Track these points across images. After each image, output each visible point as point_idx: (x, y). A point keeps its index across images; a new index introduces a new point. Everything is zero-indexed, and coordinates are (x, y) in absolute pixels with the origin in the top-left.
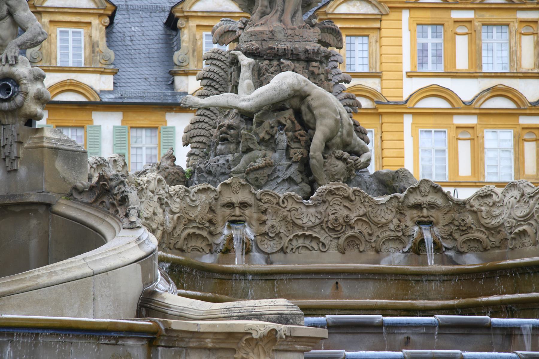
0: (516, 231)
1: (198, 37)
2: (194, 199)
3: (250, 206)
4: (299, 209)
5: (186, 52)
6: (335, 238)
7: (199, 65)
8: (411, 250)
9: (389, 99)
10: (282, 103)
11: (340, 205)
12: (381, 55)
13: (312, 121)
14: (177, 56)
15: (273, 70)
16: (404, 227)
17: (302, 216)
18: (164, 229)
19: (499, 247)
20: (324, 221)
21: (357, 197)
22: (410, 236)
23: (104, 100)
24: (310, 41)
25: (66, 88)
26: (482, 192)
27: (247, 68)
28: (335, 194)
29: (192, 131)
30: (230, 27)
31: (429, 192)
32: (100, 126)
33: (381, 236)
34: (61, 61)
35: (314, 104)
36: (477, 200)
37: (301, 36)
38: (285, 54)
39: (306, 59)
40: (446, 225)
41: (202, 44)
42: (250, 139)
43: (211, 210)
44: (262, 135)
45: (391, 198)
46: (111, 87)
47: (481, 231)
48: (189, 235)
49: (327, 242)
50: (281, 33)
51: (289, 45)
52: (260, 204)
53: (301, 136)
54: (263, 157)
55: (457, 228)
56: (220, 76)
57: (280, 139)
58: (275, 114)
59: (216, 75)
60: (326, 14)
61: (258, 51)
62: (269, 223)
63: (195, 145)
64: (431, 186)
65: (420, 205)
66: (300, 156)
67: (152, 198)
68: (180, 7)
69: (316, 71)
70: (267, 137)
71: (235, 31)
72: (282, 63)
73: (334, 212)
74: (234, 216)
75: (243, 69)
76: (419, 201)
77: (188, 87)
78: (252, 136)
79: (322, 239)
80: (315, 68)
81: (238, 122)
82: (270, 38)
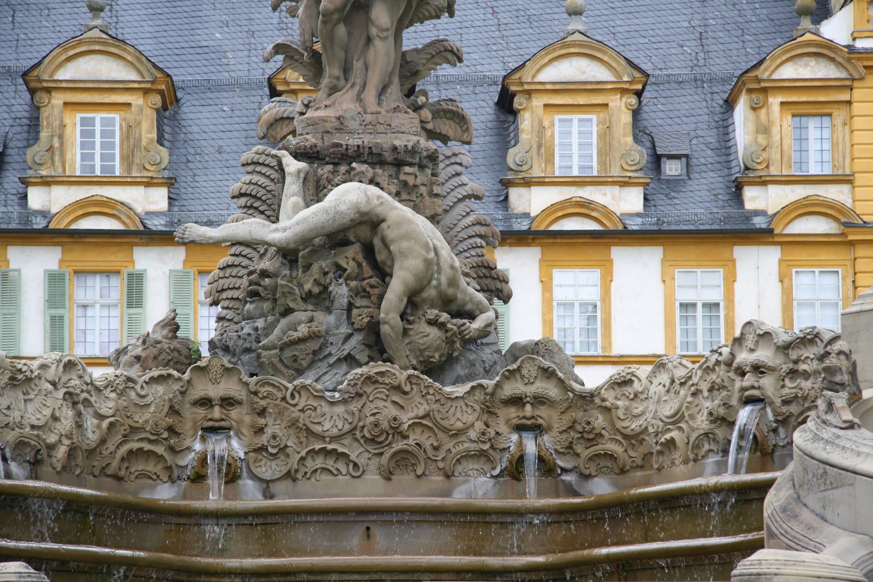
0: (663, 440)
1: (546, 123)
2: (143, 393)
3: (239, 403)
4: (319, 407)
5: (527, 149)
6: (376, 454)
7: (549, 169)
8: (506, 472)
9: (866, 218)
10: (342, 234)
11: (386, 401)
12: (852, 146)
13: (389, 263)
14: (514, 156)
15: (339, 180)
16: (493, 433)
17: (323, 419)
18: (73, 443)
19: (642, 467)
20: (358, 427)
21: (414, 386)
22: (504, 449)
24: (403, 133)
26: (618, 377)
27: (294, 178)
29: (220, 281)
30: (285, 111)
31: (536, 377)
33: (454, 451)
35: (391, 234)
36: (612, 390)
37: (387, 125)
38: (358, 155)
39: (395, 162)
40: (564, 431)
41: (553, 135)
42: (290, 293)
43: (173, 411)
44: (307, 286)
45: (473, 388)
47: (617, 441)
48: (131, 451)
49: (361, 461)
50: (356, 120)
51: (367, 140)
52: (256, 399)
53: (372, 287)
54: (308, 323)
55: (579, 436)
56: (267, 190)
57: (337, 293)
58: (333, 252)
59: (261, 189)
60: (758, 80)
61: (315, 150)
62: (269, 431)
63: (226, 303)
64: (539, 367)
65: (521, 399)
66: (366, 320)
67: (51, 392)
68: (517, 76)
69: (411, 180)
70: (316, 290)
71: (293, 118)
72: (353, 169)
73: (375, 411)
74: (210, 420)
75: (288, 180)
76: (518, 392)
77: (530, 206)
78: (292, 288)
79: (353, 457)
80: (410, 176)
81: (278, 264)
82: (336, 129)
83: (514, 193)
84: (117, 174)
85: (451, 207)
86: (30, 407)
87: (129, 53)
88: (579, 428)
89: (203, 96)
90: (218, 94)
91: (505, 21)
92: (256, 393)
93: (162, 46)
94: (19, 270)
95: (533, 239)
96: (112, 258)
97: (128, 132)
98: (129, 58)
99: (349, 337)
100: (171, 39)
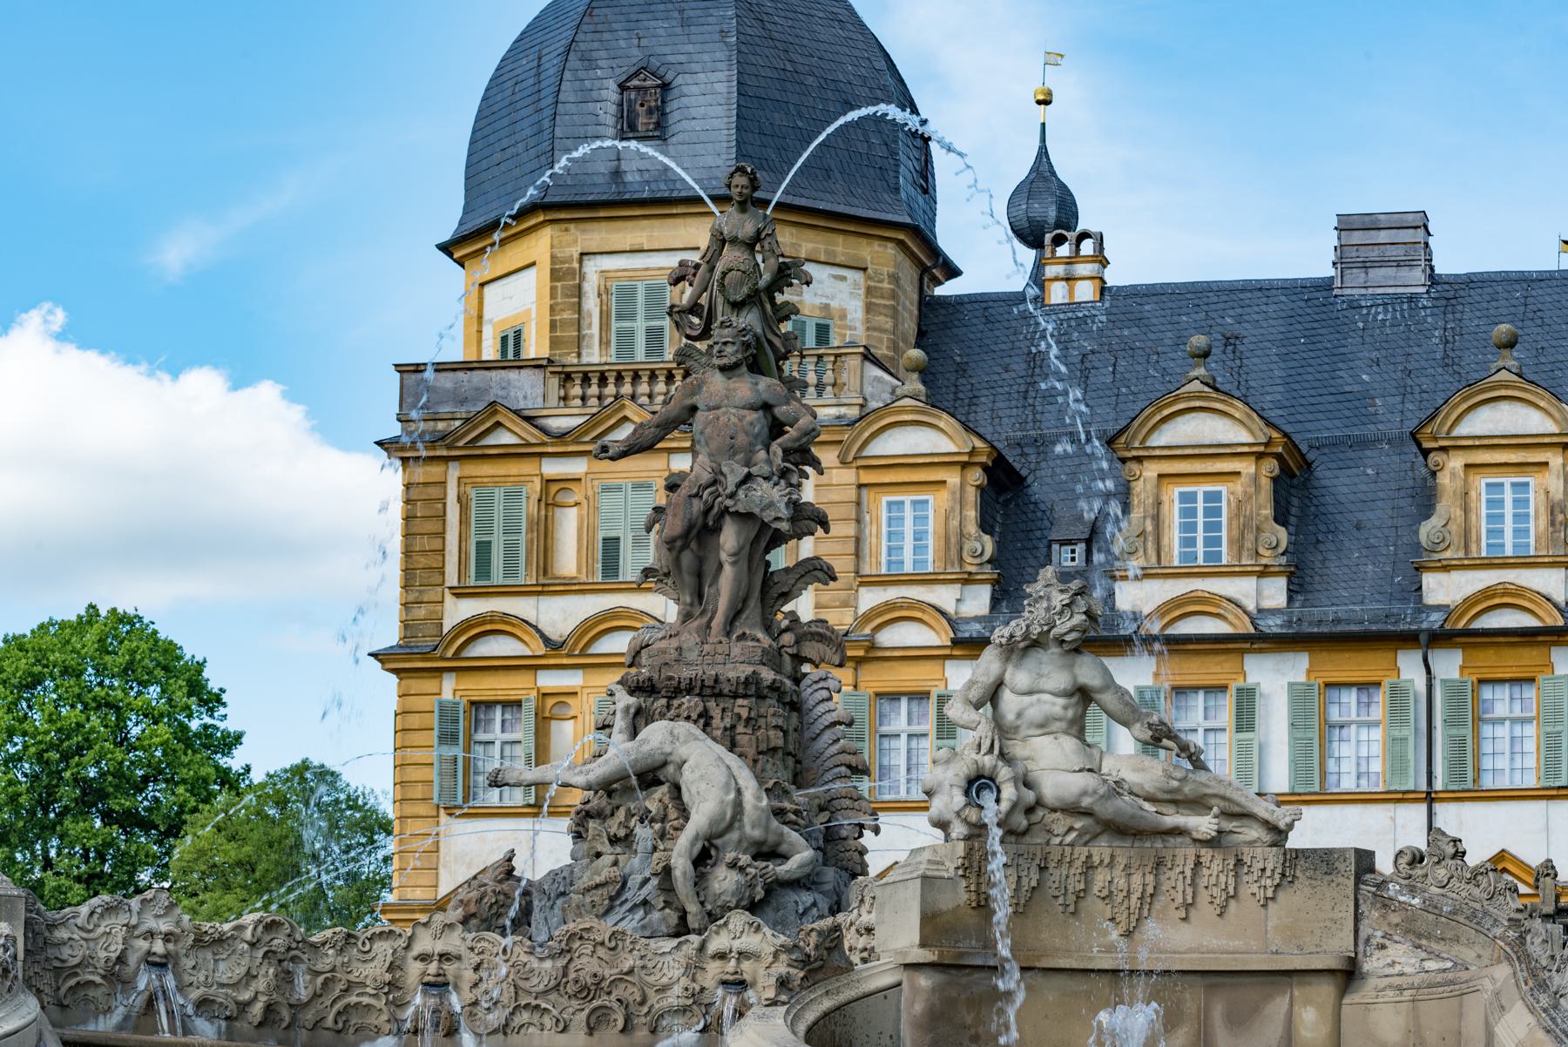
2: (367, 948)
16: (698, 988)
25: (1497, 601)
28: (581, 938)
33: (657, 1006)
34: (1488, 545)
45: (680, 943)
52: (472, 955)
53: (676, 829)
62: (483, 986)
66: (661, 865)
70: (622, 833)
84: (1224, 562)
85: (818, 735)
86: (222, 966)
87: (1236, 408)
89: (1341, 456)
90: (1360, 454)
92: (472, 949)
93: (1295, 394)
96: (1217, 669)
97: (1239, 508)
98: (1237, 415)
99: (646, 881)
100: (1306, 385)
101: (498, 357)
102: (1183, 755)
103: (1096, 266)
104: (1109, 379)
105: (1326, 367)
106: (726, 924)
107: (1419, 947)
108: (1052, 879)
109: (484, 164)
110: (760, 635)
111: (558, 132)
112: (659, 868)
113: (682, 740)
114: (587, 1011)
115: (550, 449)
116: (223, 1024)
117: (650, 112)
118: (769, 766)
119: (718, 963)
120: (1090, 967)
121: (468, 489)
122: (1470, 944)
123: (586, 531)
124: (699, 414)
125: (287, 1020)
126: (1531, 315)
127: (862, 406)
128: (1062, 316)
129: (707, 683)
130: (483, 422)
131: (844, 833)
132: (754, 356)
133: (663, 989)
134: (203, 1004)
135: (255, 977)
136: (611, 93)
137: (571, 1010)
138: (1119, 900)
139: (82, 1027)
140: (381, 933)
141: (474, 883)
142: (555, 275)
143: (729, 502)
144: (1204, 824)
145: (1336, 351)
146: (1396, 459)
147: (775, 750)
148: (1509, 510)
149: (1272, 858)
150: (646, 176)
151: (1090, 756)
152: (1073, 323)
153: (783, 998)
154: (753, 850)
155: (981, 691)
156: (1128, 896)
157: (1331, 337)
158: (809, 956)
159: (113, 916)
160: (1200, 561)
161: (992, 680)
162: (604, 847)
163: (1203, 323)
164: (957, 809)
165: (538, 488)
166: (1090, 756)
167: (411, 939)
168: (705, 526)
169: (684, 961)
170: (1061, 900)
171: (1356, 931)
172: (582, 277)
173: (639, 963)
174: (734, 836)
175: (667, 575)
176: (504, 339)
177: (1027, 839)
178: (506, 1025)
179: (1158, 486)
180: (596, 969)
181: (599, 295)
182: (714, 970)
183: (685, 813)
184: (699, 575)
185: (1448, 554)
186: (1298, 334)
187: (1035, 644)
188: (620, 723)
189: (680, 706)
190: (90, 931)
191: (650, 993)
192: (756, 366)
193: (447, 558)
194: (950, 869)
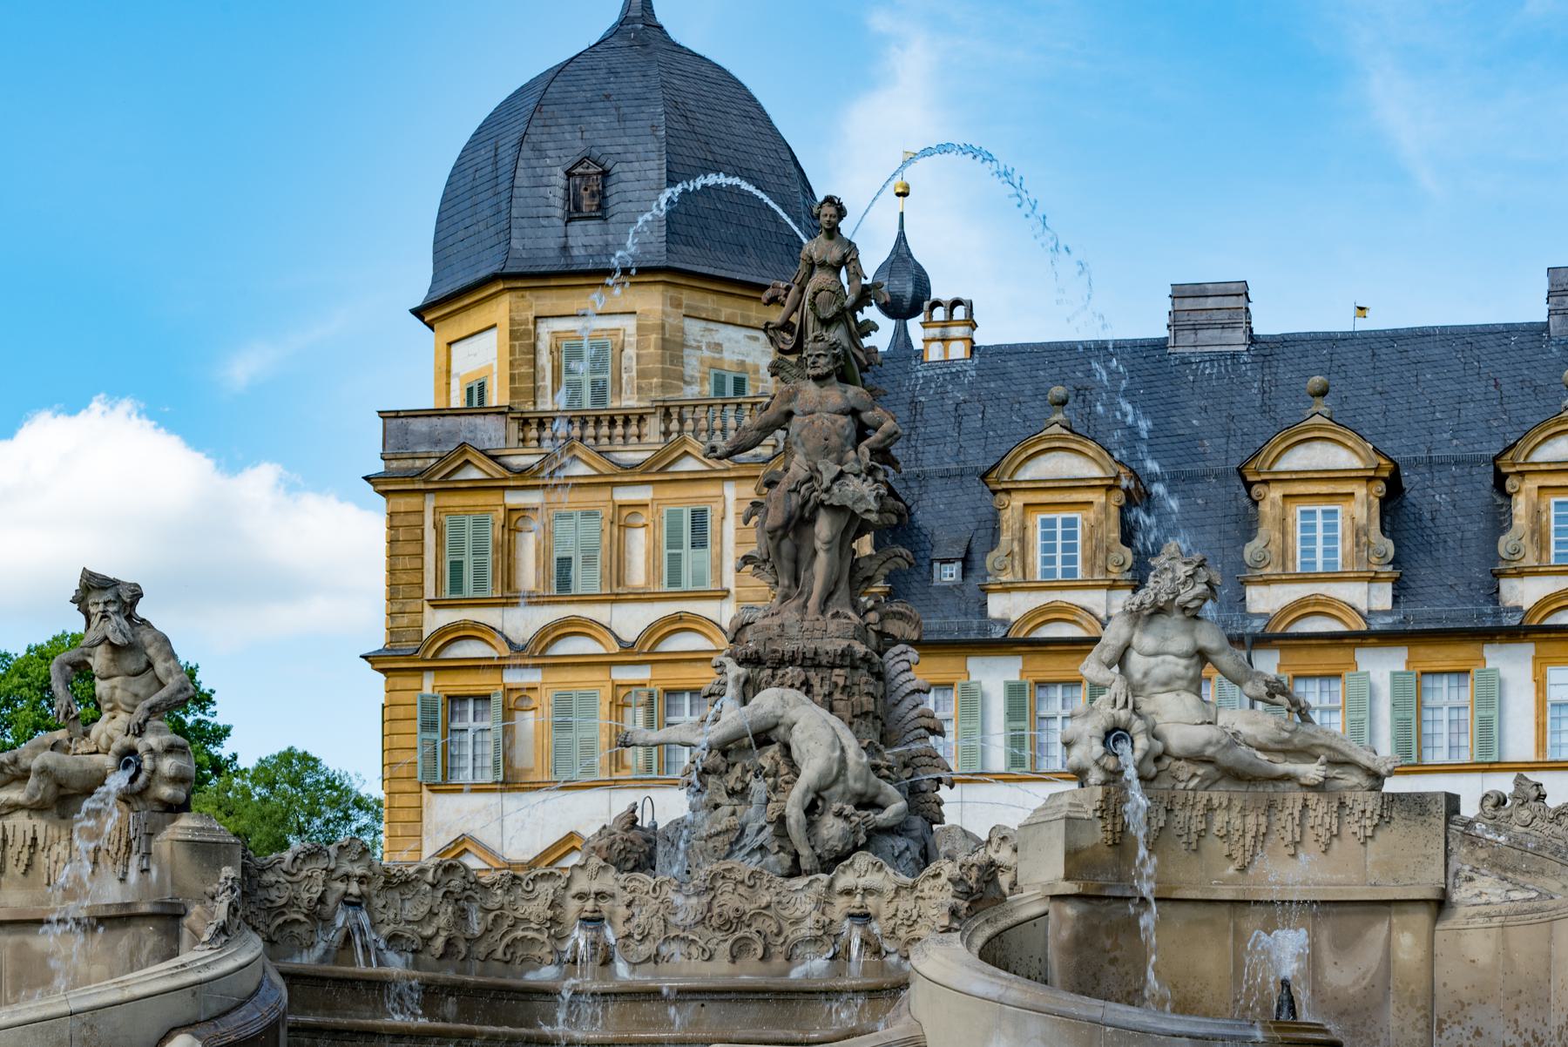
1: (1543, 507)
2: (530, 888)
7: (1544, 557)
14: (1505, 544)
16: (827, 921)
23: (1372, 628)
25: (1310, 610)
28: (723, 877)
32: (1368, 673)
34: (1302, 563)
41: (1548, 520)
46: (1388, 605)
52: (625, 893)
53: (787, 783)
62: (635, 921)
66: (776, 814)
70: (739, 786)
83: (1505, 584)
84: (1079, 577)
86: (408, 905)
87: (1090, 448)
88: (900, 914)
91: (1507, 394)
92: (624, 888)
94: (979, 683)
95: (1525, 635)
97: (1091, 532)
99: (762, 829)
101: (465, 405)
102: (1294, 709)
103: (967, 329)
104: (979, 425)
105: (1163, 414)
106: (851, 864)
107: (1505, 879)
108: (1177, 819)
109: (450, 241)
110: (851, 614)
111: (514, 213)
112: (774, 817)
113: (791, 704)
114: (730, 942)
115: (512, 483)
116: (410, 956)
117: (593, 195)
118: (863, 728)
119: (845, 899)
120: (1213, 898)
121: (443, 517)
122: (1556, 875)
123: (543, 552)
124: (795, 417)
125: (464, 951)
126: (1336, 369)
127: (774, 446)
128: (938, 371)
129: (807, 655)
130: (454, 460)
131: (924, 787)
132: (841, 366)
133: (797, 922)
134: (393, 939)
135: (436, 914)
136: (559, 179)
137: (715, 941)
138: (1236, 838)
139: (288, 960)
140: (543, 875)
141: (605, 832)
142: (513, 335)
143: (824, 496)
144: (1312, 771)
145: (1170, 400)
146: (1222, 491)
147: (865, 714)
148: (1320, 533)
149: (1371, 802)
150: (590, 250)
151: (1208, 711)
152: (948, 377)
153: (956, 925)
154: (855, 801)
155: (1113, 653)
156: (1243, 836)
157: (1166, 389)
158: (972, 888)
159: (314, 861)
160: (1059, 576)
161: (1121, 643)
162: (723, 798)
163: (1058, 377)
164: (1096, 757)
165: (502, 516)
166: (1208, 711)
167: (569, 879)
168: (802, 517)
169: (814, 897)
170: (1185, 839)
171: (1446, 865)
172: (537, 337)
173: (775, 899)
174: (839, 788)
175: (765, 561)
176: (470, 390)
177: (1155, 784)
178: (657, 955)
179: (1024, 513)
180: (738, 904)
181: (551, 352)
182: (841, 905)
183: (794, 769)
184: (796, 562)
185: (1268, 570)
186: (1138, 386)
187: (1159, 611)
188: (731, 691)
189: (784, 675)
190: (294, 875)
191: (785, 925)
192: (845, 378)
193: (425, 575)
194: (1088, 811)
